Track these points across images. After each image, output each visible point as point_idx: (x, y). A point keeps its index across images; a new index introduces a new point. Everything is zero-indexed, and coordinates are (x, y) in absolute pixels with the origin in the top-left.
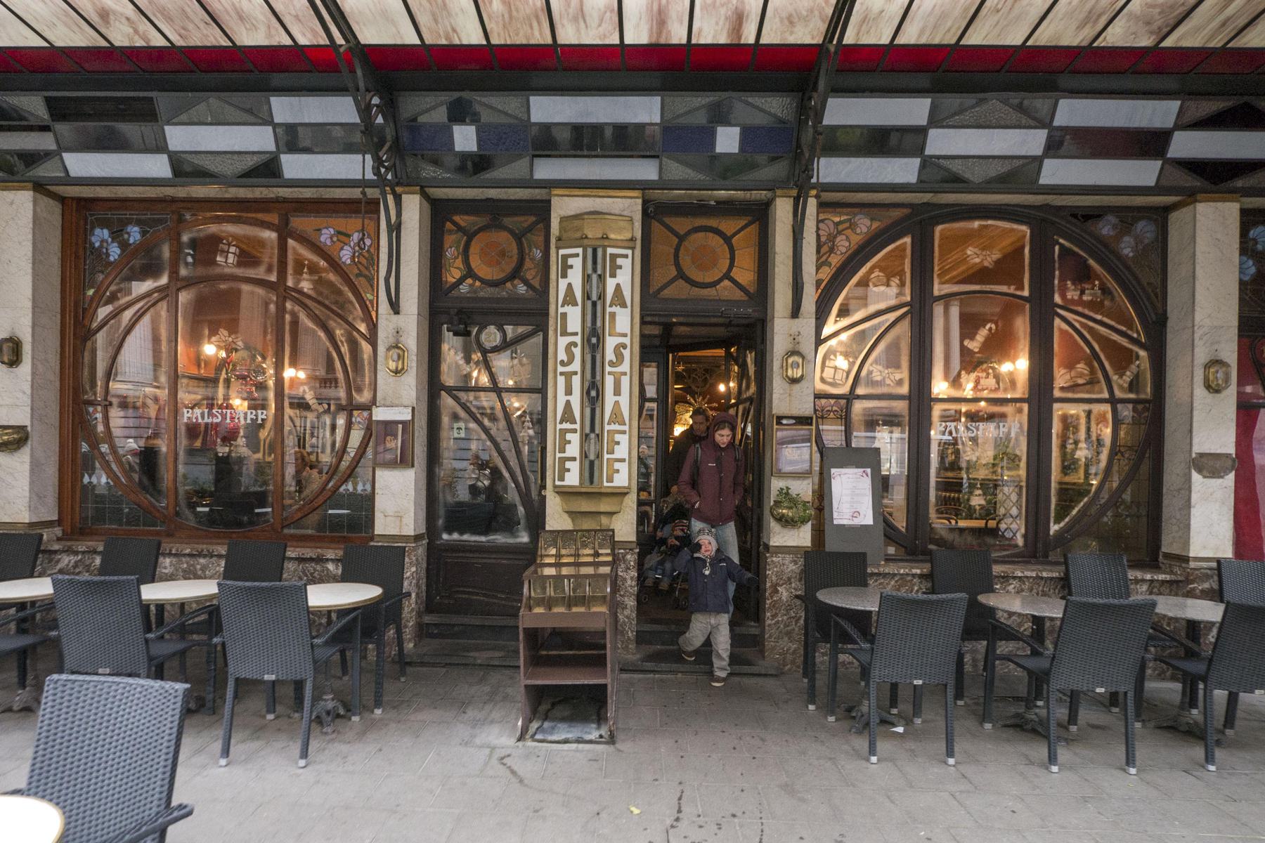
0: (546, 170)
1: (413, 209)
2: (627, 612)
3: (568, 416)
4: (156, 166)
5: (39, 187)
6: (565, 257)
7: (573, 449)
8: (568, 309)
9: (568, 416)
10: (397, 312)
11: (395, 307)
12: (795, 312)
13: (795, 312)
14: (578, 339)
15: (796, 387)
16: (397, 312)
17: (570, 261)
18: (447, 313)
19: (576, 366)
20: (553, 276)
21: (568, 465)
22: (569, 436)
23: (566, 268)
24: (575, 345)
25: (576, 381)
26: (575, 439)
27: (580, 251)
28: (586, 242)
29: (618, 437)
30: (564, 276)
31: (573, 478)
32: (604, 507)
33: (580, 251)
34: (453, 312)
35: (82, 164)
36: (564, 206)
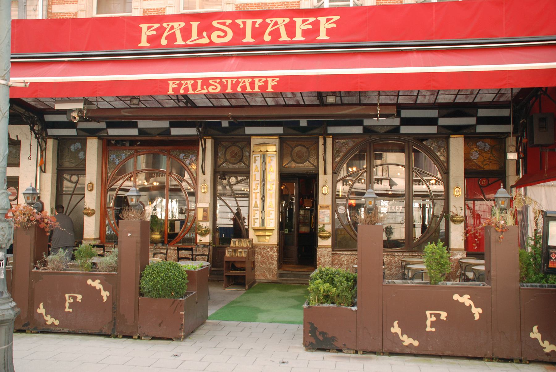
0: (249, 130)
1: (209, 143)
2: (274, 266)
3: (256, 206)
4: (134, 132)
5: (100, 138)
6: (255, 157)
7: (258, 216)
8: (256, 173)
9: (256, 206)
10: (204, 174)
11: (204, 173)
12: (325, 173)
13: (325, 173)
14: (259, 182)
15: (326, 196)
16: (204, 174)
17: (257, 158)
18: (219, 174)
19: (258, 190)
20: (251, 163)
21: (256, 220)
22: (256, 212)
23: (255, 161)
24: (258, 184)
25: (259, 194)
26: (258, 213)
27: (259, 155)
28: (261, 153)
29: (271, 212)
30: (255, 163)
31: (257, 225)
32: (267, 233)
33: (259, 155)
34: (221, 172)
35: (113, 132)
36: (254, 141)
